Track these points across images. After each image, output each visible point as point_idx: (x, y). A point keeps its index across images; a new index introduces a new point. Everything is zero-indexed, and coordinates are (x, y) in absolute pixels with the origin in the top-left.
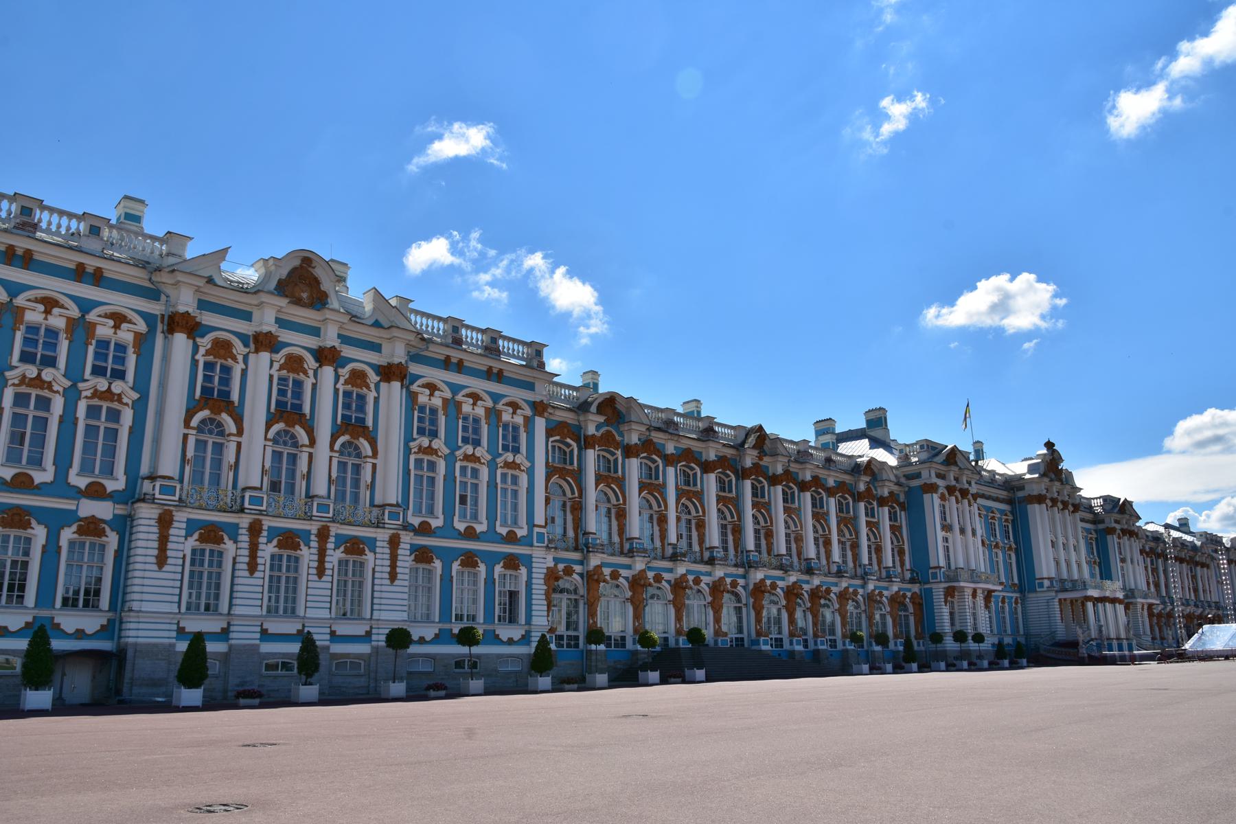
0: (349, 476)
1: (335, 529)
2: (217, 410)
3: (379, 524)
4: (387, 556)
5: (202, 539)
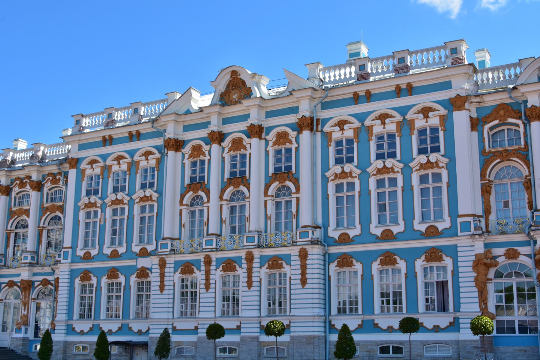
0: (284, 210)
1: (257, 253)
2: (195, 191)
3: (294, 243)
4: (299, 267)
5: (183, 272)
